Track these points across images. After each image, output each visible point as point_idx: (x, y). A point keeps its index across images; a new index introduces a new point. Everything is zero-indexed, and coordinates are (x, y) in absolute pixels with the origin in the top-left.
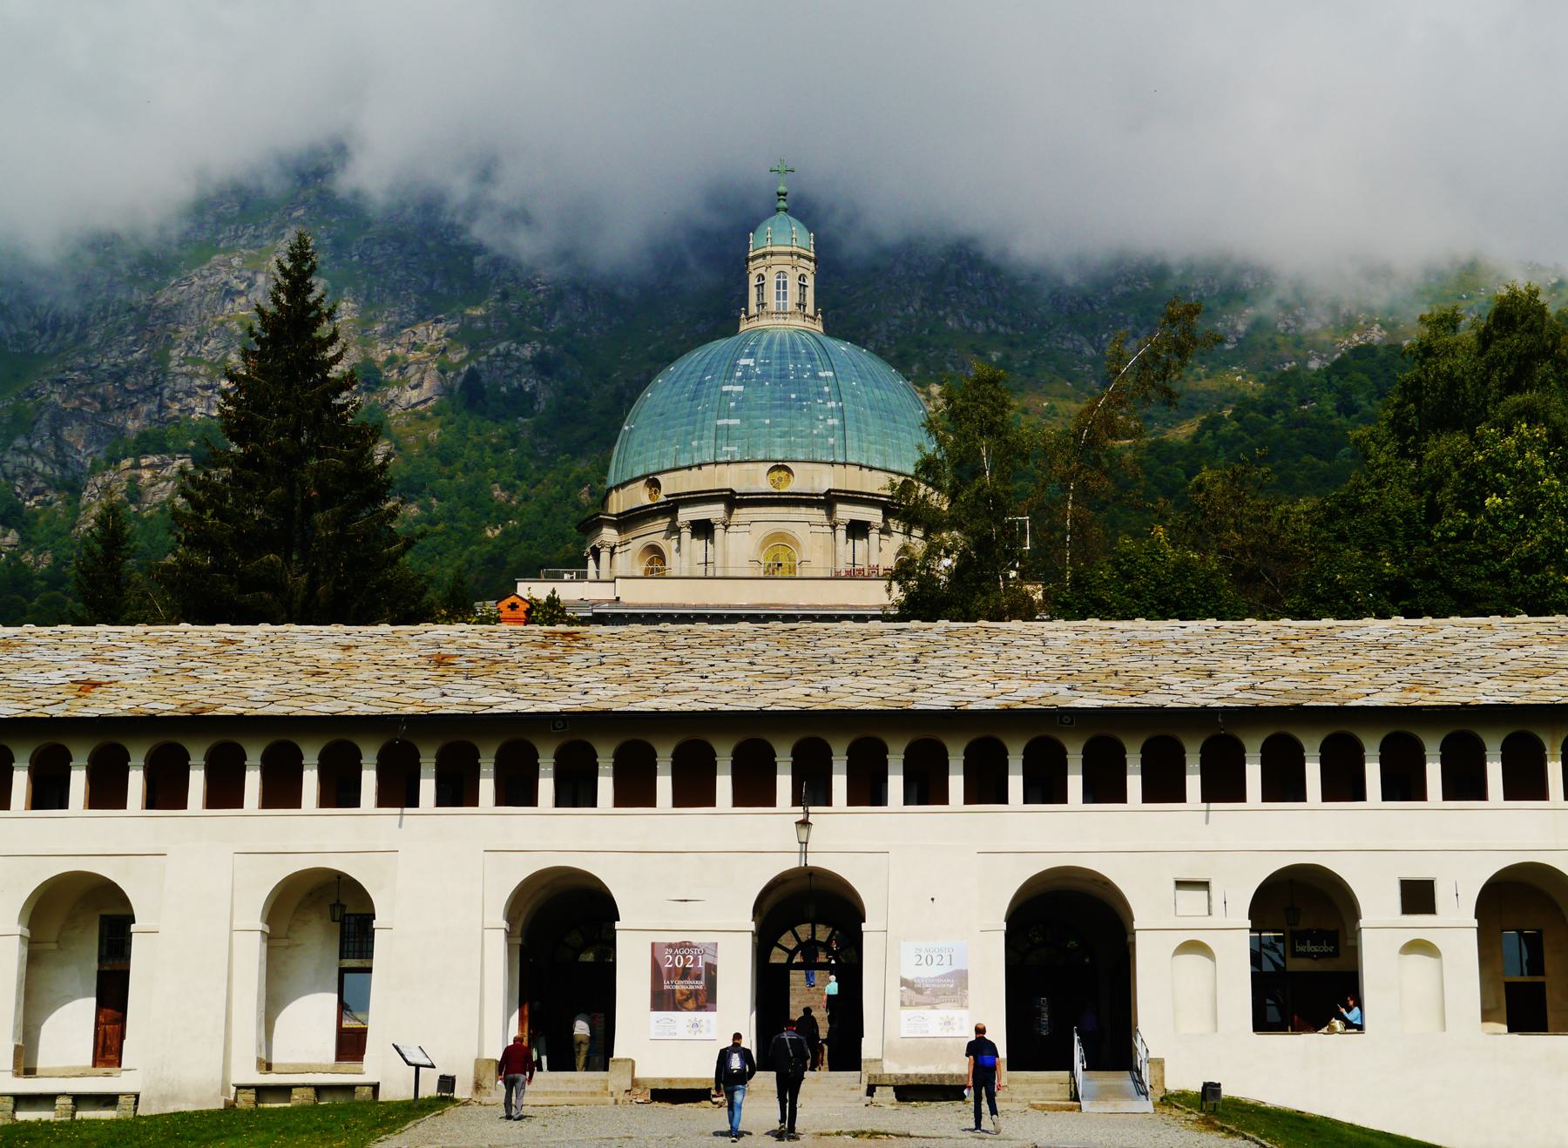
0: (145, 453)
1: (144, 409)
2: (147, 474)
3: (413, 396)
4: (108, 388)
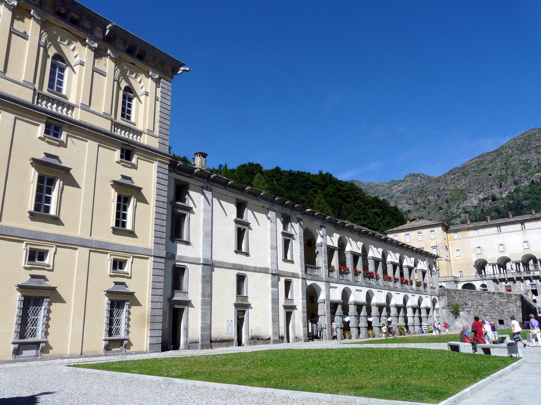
0: (485, 201)
1: (482, 194)
2: (486, 203)
3: (523, 184)
4: (476, 192)
